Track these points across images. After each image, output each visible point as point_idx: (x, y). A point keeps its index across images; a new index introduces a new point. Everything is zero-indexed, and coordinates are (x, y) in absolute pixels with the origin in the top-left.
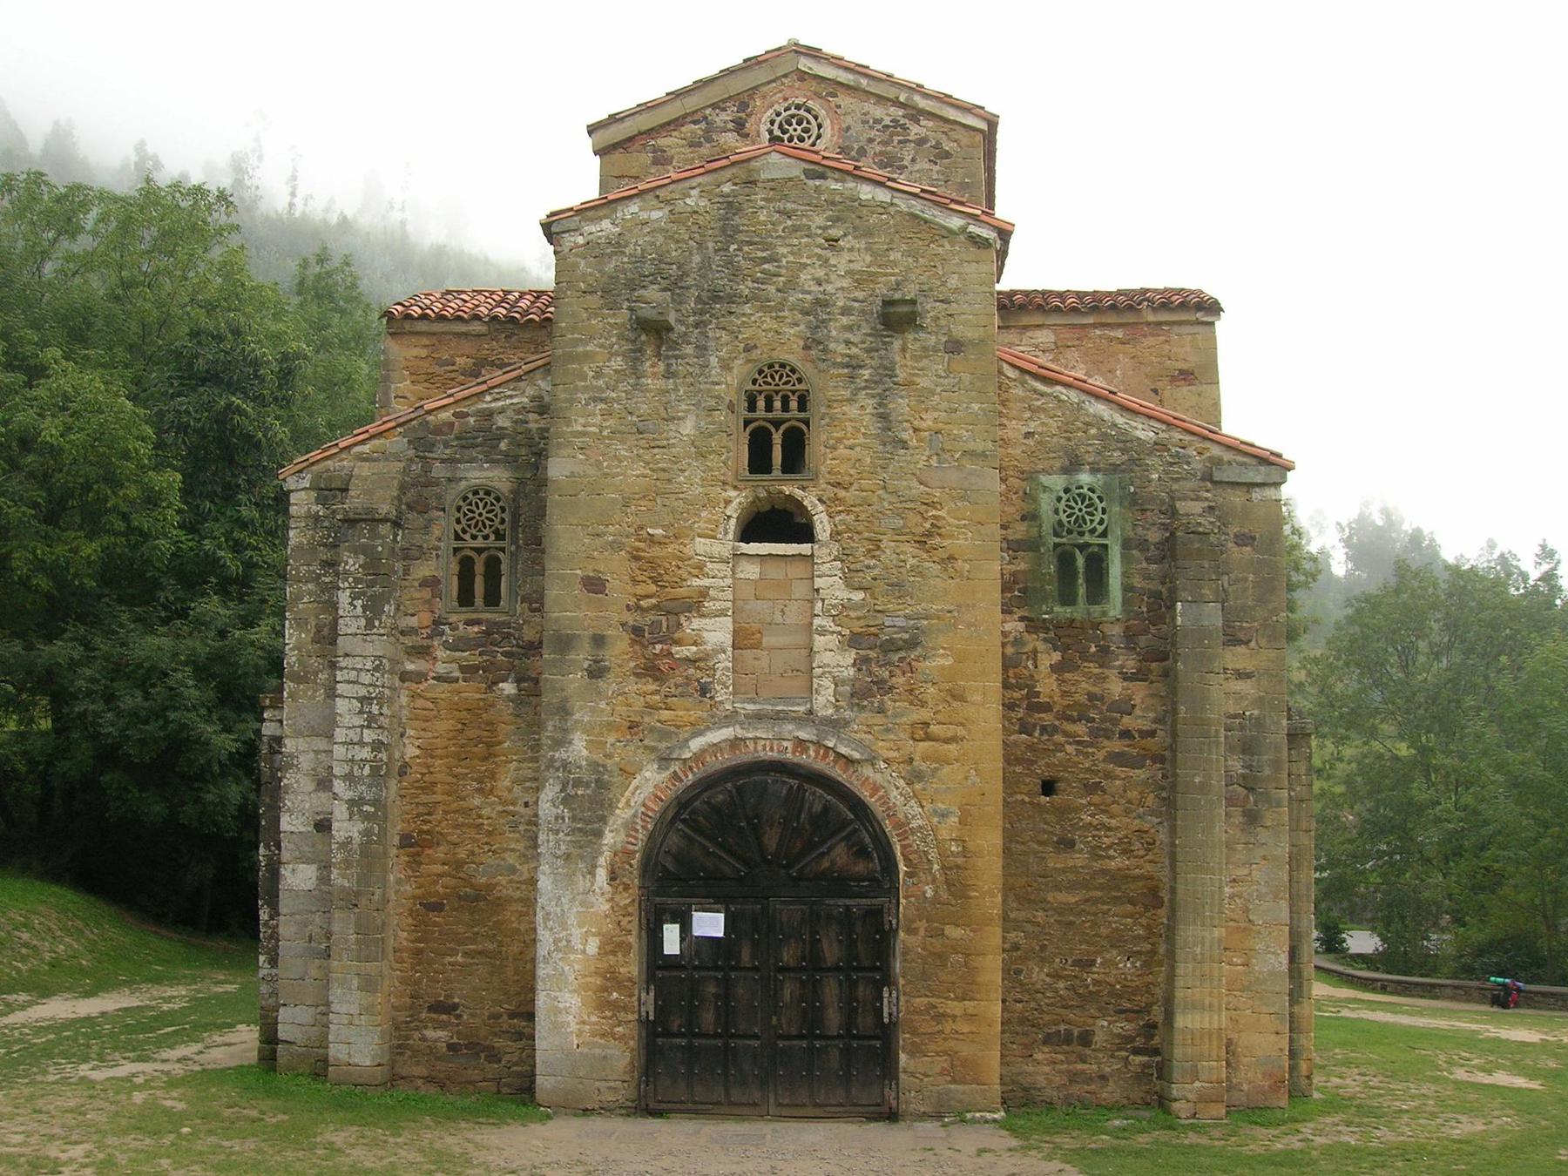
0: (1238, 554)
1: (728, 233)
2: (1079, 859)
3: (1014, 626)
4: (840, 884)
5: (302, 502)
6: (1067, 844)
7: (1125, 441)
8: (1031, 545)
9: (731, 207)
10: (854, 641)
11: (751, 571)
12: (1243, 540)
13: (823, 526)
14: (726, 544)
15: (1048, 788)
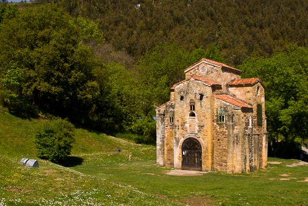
0: (236, 116)
1: (188, 86)
2: (221, 147)
3: (215, 124)
4: (197, 149)
5: (157, 112)
6: (220, 146)
7: (226, 105)
8: (217, 116)
9: (189, 84)
10: (199, 126)
11: (190, 119)
12: (237, 115)
13: (196, 115)
14: (188, 117)
15: (219, 140)
